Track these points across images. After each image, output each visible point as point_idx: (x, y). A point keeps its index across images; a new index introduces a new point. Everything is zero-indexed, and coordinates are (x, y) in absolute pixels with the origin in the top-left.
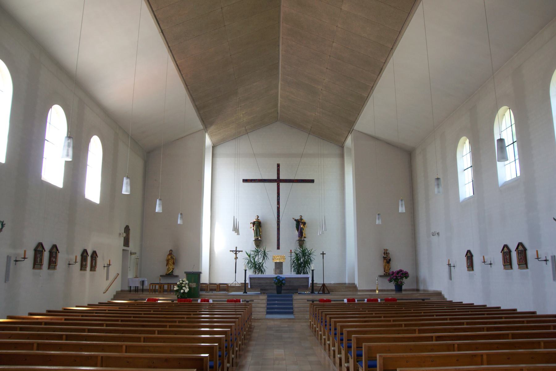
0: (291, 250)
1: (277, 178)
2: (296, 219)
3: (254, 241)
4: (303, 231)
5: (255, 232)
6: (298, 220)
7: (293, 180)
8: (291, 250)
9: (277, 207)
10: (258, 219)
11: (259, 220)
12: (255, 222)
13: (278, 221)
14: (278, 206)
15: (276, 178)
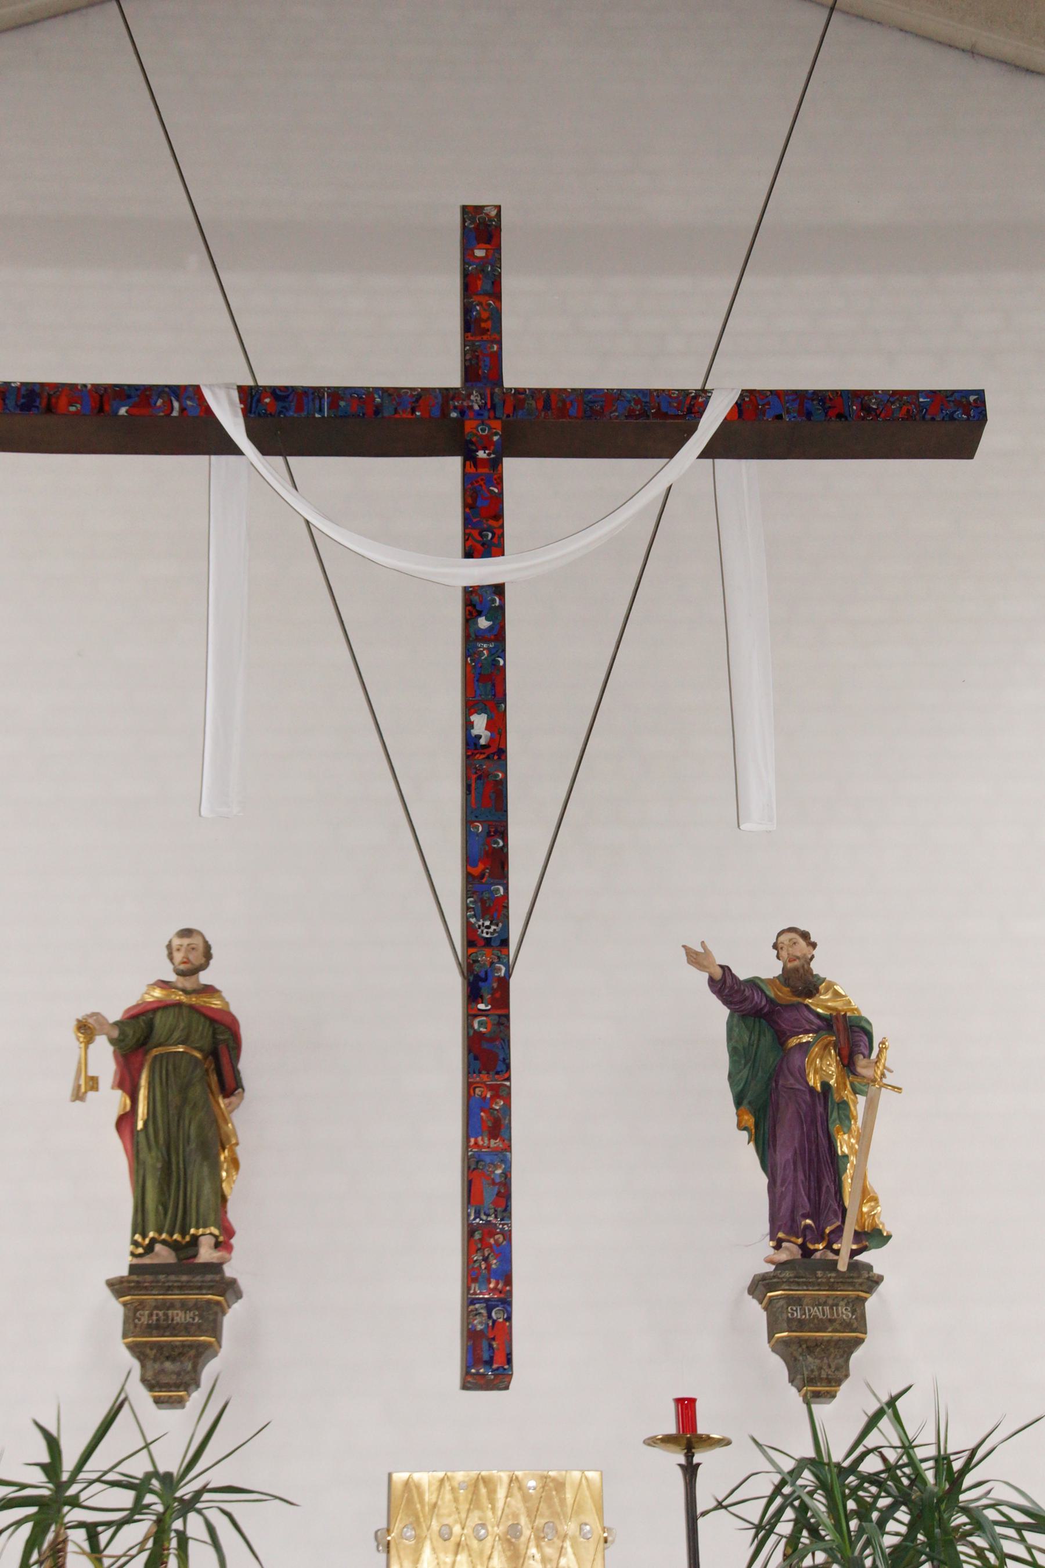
0: (686, 1408)
1: (470, 372)
2: (743, 973)
3: (117, 1287)
4: (844, 1144)
5: (152, 1159)
6: (753, 983)
7: (685, 393)
8: (686, 1408)
9: (470, 743)
10: (205, 978)
11: (209, 990)
12: (159, 1019)
13: (487, 929)
14: (480, 722)
15: (452, 378)
